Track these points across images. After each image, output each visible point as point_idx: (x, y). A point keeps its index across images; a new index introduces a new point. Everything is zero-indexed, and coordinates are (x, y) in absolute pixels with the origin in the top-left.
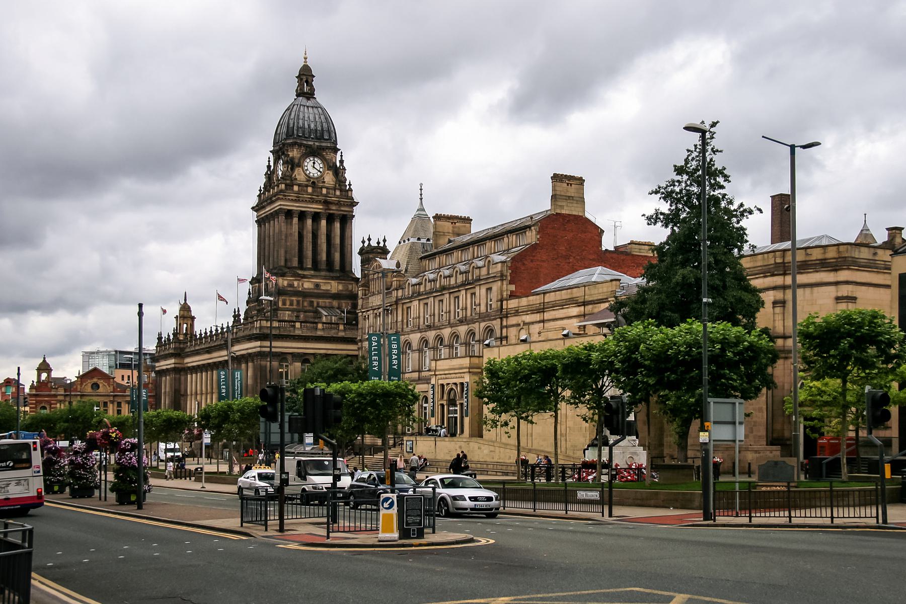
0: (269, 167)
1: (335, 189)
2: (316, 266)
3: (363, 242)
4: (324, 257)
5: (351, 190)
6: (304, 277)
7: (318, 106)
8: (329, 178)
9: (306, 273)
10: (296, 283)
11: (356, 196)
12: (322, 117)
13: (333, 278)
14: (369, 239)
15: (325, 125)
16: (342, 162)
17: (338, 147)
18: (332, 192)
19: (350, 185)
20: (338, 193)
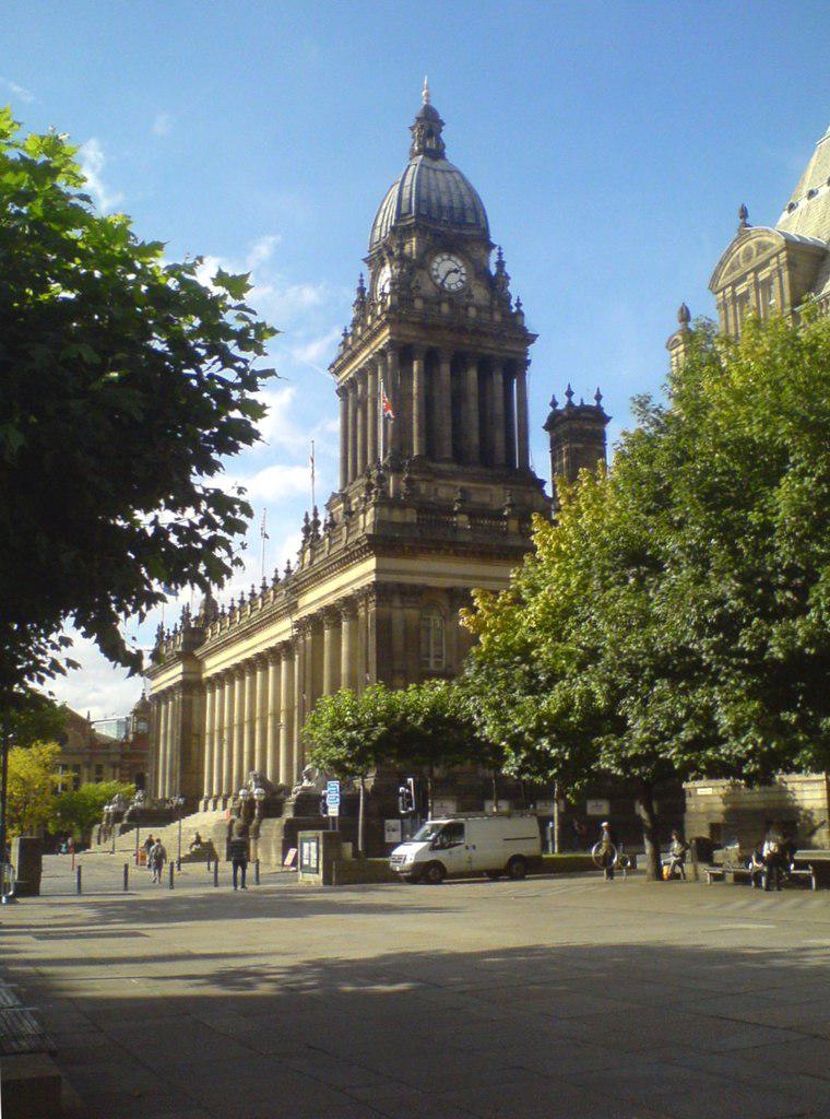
0: (361, 290)
1: (491, 310)
2: (459, 456)
3: (554, 404)
4: (475, 438)
5: (520, 313)
6: (440, 475)
7: (452, 171)
8: (480, 294)
9: (445, 467)
10: (423, 487)
11: (531, 323)
12: (462, 186)
13: (495, 480)
14: (569, 393)
15: (467, 200)
16: (500, 264)
17: (493, 240)
18: (486, 316)
19: (518, 305)
20: (498, 317)
